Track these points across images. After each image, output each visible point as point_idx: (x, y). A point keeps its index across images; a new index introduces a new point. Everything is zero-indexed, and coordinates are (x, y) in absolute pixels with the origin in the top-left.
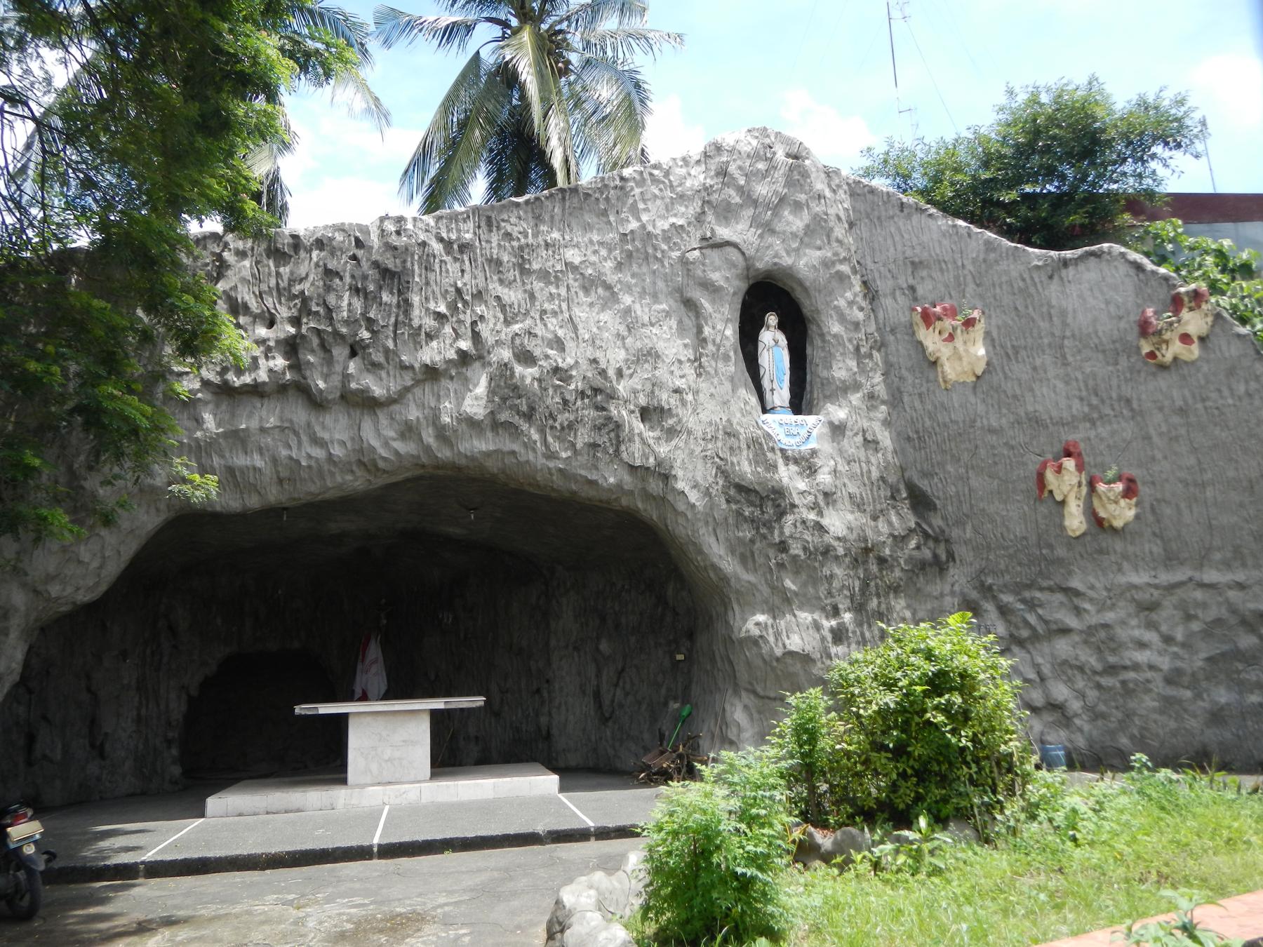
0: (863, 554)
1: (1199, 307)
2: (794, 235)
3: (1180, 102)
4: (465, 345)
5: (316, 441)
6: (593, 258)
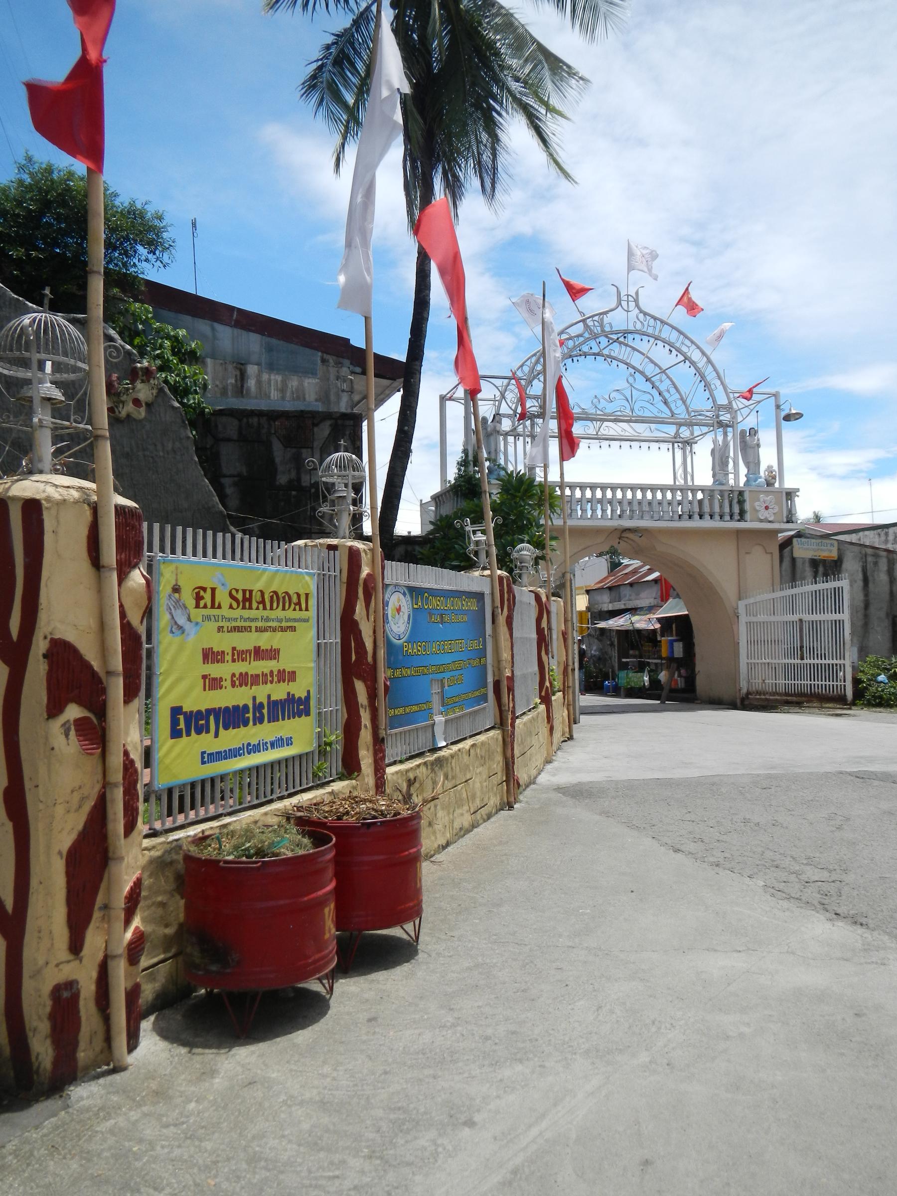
1: (149, 381)
3: (160, 218)
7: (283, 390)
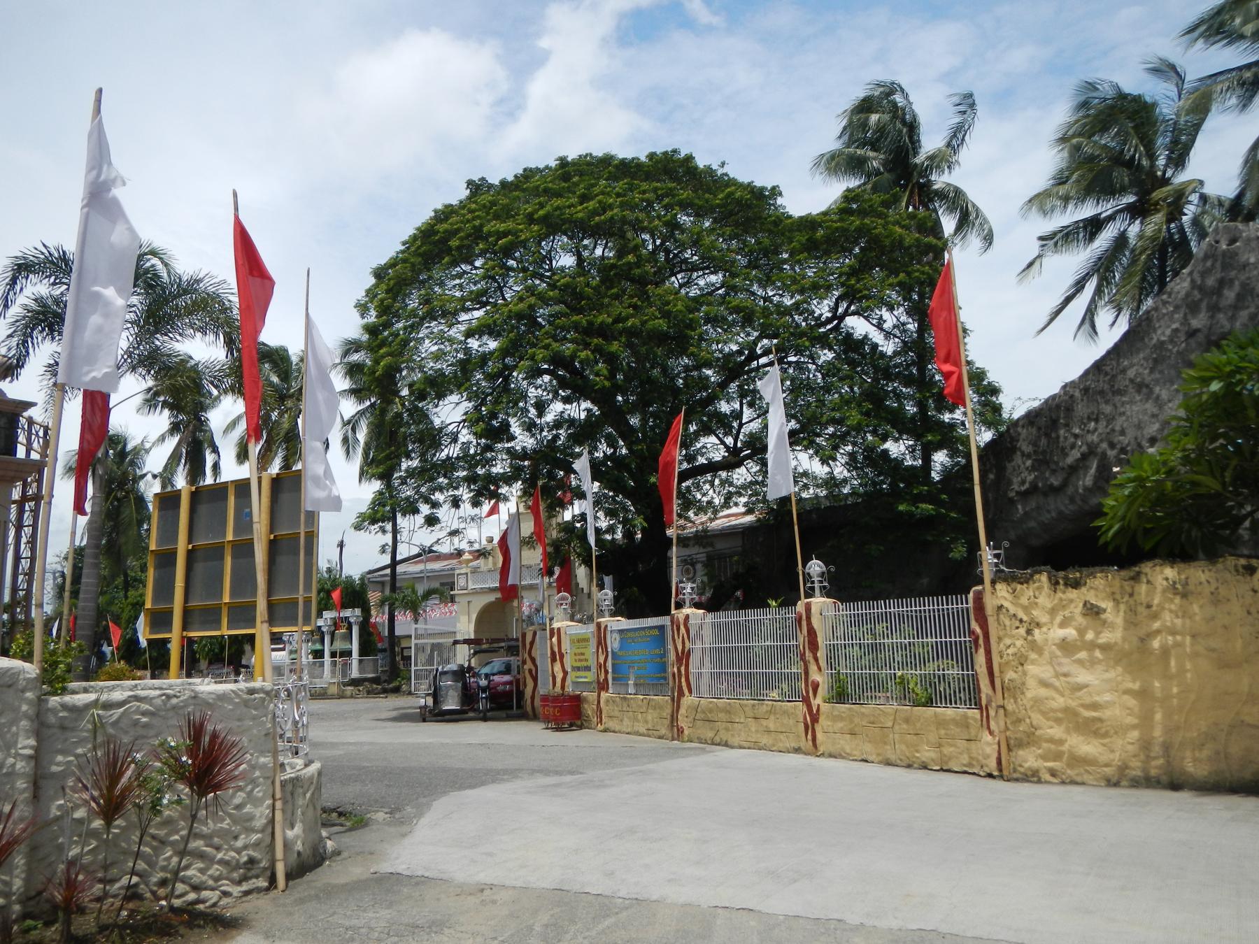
2: (1230, 306)
4: (1084, 448)
5: (1049, 512)
6: (1141, 370)
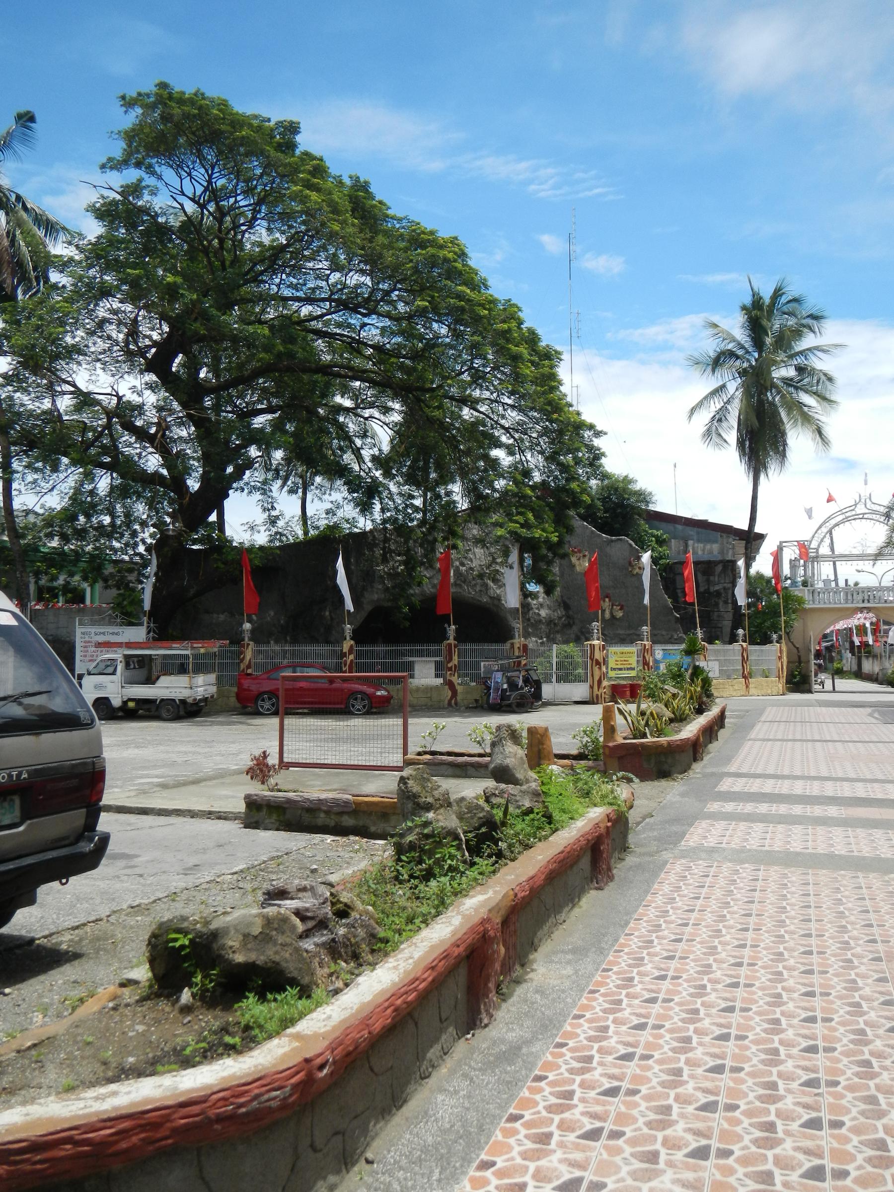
0: (550, 622)
7: (703, 550)
